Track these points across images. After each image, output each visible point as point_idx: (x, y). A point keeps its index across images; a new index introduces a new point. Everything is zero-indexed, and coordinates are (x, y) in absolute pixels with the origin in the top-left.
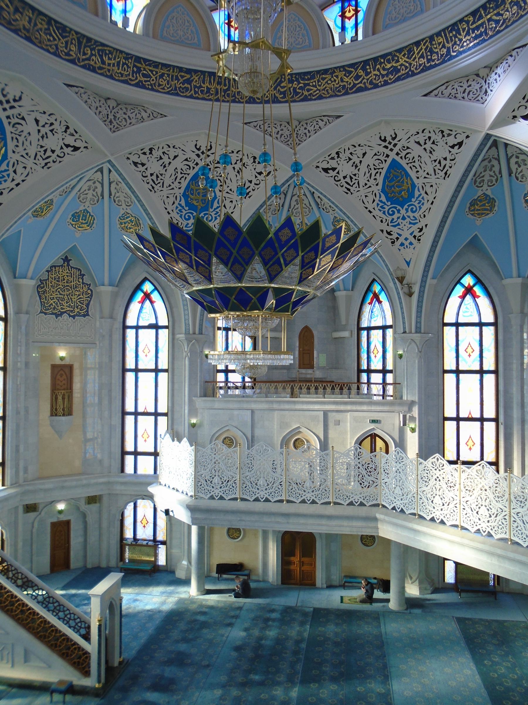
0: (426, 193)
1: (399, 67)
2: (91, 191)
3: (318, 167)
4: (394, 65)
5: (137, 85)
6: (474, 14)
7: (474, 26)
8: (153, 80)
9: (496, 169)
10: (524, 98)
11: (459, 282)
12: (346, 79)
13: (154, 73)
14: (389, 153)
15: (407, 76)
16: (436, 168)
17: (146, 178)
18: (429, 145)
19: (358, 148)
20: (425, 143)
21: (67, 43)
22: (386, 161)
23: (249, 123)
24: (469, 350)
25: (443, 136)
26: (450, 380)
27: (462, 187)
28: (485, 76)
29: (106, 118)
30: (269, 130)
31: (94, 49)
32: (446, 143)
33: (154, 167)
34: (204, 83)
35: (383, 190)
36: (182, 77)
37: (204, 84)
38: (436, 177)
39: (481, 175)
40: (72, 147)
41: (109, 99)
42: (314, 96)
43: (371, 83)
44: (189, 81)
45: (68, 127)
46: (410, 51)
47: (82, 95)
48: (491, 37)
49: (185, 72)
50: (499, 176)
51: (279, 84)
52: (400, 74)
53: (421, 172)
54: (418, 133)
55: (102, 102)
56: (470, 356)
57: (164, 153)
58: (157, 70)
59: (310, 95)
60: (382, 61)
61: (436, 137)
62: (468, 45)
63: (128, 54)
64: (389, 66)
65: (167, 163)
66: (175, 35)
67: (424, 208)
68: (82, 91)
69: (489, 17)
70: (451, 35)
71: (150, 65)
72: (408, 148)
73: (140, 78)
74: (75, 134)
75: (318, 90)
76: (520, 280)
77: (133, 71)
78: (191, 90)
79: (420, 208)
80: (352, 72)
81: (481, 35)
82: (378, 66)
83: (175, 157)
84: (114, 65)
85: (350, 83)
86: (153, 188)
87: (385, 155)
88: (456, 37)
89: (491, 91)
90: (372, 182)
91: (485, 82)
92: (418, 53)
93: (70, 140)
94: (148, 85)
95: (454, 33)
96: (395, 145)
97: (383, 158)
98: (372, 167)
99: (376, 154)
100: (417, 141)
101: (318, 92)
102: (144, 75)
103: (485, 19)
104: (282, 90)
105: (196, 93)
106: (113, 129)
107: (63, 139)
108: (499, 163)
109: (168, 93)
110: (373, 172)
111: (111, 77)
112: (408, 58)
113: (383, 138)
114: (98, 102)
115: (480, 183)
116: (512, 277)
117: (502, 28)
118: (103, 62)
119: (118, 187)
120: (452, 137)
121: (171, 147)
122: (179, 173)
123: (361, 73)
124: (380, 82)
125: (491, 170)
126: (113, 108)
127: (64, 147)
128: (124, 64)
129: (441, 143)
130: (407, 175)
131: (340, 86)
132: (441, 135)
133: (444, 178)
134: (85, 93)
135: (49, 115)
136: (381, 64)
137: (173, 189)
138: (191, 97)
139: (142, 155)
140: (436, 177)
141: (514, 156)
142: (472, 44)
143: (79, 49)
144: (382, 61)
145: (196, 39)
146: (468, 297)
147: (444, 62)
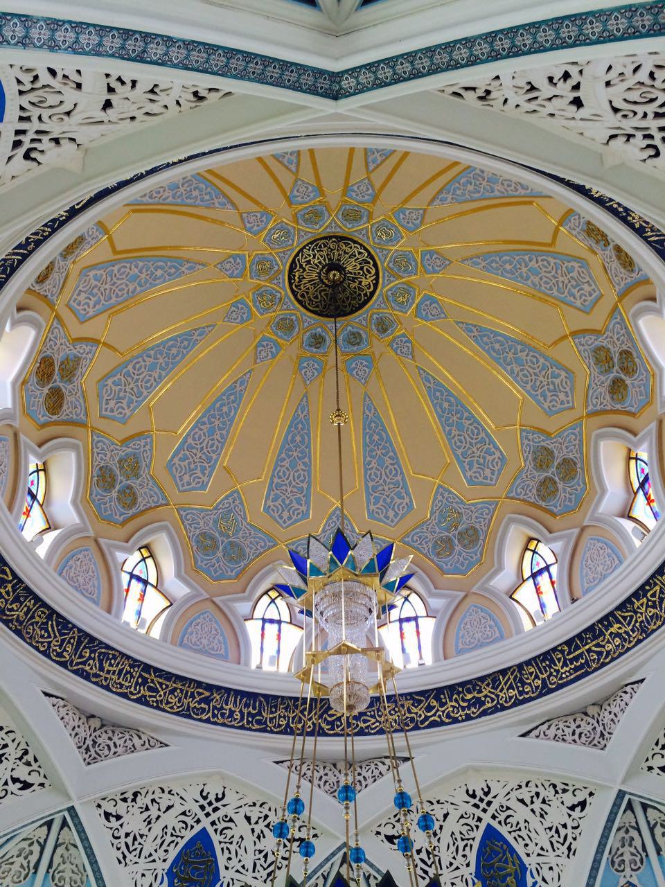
0: (544, 880)
1: (483, 699)
2: (21, 859)
3: (378, 833)
4: (477, 695)
5: (138, 701)
6: (568, 643)
7: (571, 656)
8: (160, 696)
9: (638, 843)
10: (657, 744)
12: (415, 710)
13: (164, 686)
14: (482, 815)
15: (495, 710)
16: (553, 840)
17: (118, 841)
18: (537, 805)
19: (436, 806)
20: (532, 802)
21: (63, 641)
22: (477, 827)
23: (282, 762)
25: (557, 792)
27: (597, 870)
28: (596, 716)
29: (82, 744)
30: (309, 773)
31: (94, 652)
32: (562, 803)
33: (133, 822)
34: (227, 704)
35: (478, 875)
36: (199, 694)
37: (227, 704)
38: (558, 852)
39: (619, 853)
40: (21, 782)
41: (93, 716)
42: (372, 729)
43: (448, 716)
44: (207, 701)
45: (26, 752)
46: (494, 681)
47: (61, 709)
48: (596, 670)
49: (205, 689)
50: (644, 855)
51: (326, 712)
52: (485, 707)
53: (532, 845)
54: (520, 787)
55: (82, 721)
57: (153, 801)
58: (168, 683)
59: (367, 727)
60: (461, 689)
62: (567, 676)
63: (135, 660)
64: (469, 697)
65: (154, 817)
66: (198, 643)
68: (62, 703)
69: (587, 647)
70: (544, 665)
71: (160, 676)
72: (508, 808)
73: (144, 691)
74: (33, 763)
75: (377, 721)
77: (137, 683)
78: (209, 712)
80: (422, 701)
81: (582, 666)
82: (455, 696)
83: (169, 808)
84: (114, 673)
85: (420, 716)
86: (125, 857)
87: (476, 818)
88: (550, 667)
89: (609, 733)
90: (460, 860)
91: (598, 722)
92: (506, 684)
93: (22, 772)
94: (153, 701)
95: (548, 663)
96: (489, 803)
97: (473, 823)
98: (458, 836)
99: (462, 817)
100: (520, 798)
101: (378, 724)
102: (150, 689)
103: (583, 649)
104: (329, 719)
105: (214, 716)
106: (87, 760)
107: (13, 769)
108: (640, 835)
109: (177, 714)
110: (461, 844)
111: (107, 688)
112: (493, 688)
113: (471, 793)
114: (77, 720)
115: (620, 866)
117: (607, 660)
118: (102, 669)
119: (66, 854)
120: (570, 794)
121: (166, 792)
122: (169, 834)
123: (434, 703)
124: (461, 716)
125: (630, 845)
126: (95, 731)
127: (10, 782)
128: (127, 672)
129: (555, 802)
130: (512, 851)
131: (407, 718)
132: (553, 792)
133: (568, 856)
134: (65, 706)
135: (6, 733)
136: (459, 693)
137: (154, 861)
138: (208, 721)
139: (120, 803)
140: (558, 852)
141: (659, 825)
142: (572, 677)
143: (76, 650)
144: (461, 689)
145: (223, 650)
147: (541, 695)
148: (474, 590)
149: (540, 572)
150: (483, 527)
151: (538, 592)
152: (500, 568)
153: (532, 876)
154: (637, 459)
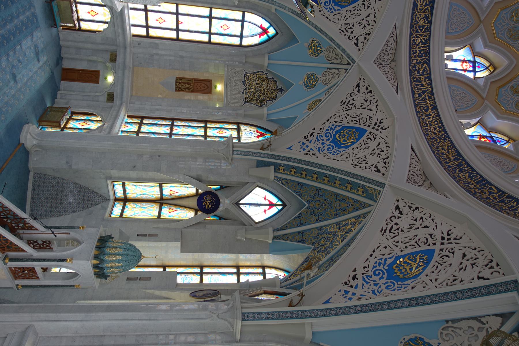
11: (271, 25)
18: (364, 23)
20: (366, 21)
24: (225, 27)
26: (205, 11)
53: (349, 14)
54: (375, 17)
56: (222, 27)
61: (368, 29)
67: (326, 11)
72: (368, 7)
76: (266, 64)
79: (326, 9)
116: (269, 60)
132: (368, 32)
146: (260, 30)
148: (482, 25)
149: (474, 67)
150: (517, 45)
151: (464, 61)
152: (486, 46)
153: (338, 10)
154: (507, 142)
